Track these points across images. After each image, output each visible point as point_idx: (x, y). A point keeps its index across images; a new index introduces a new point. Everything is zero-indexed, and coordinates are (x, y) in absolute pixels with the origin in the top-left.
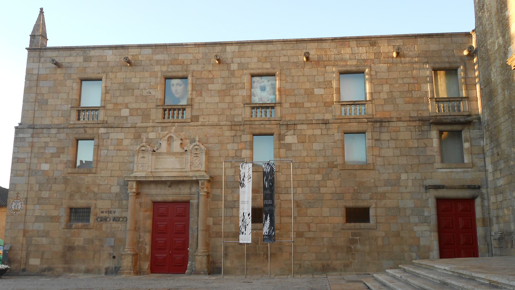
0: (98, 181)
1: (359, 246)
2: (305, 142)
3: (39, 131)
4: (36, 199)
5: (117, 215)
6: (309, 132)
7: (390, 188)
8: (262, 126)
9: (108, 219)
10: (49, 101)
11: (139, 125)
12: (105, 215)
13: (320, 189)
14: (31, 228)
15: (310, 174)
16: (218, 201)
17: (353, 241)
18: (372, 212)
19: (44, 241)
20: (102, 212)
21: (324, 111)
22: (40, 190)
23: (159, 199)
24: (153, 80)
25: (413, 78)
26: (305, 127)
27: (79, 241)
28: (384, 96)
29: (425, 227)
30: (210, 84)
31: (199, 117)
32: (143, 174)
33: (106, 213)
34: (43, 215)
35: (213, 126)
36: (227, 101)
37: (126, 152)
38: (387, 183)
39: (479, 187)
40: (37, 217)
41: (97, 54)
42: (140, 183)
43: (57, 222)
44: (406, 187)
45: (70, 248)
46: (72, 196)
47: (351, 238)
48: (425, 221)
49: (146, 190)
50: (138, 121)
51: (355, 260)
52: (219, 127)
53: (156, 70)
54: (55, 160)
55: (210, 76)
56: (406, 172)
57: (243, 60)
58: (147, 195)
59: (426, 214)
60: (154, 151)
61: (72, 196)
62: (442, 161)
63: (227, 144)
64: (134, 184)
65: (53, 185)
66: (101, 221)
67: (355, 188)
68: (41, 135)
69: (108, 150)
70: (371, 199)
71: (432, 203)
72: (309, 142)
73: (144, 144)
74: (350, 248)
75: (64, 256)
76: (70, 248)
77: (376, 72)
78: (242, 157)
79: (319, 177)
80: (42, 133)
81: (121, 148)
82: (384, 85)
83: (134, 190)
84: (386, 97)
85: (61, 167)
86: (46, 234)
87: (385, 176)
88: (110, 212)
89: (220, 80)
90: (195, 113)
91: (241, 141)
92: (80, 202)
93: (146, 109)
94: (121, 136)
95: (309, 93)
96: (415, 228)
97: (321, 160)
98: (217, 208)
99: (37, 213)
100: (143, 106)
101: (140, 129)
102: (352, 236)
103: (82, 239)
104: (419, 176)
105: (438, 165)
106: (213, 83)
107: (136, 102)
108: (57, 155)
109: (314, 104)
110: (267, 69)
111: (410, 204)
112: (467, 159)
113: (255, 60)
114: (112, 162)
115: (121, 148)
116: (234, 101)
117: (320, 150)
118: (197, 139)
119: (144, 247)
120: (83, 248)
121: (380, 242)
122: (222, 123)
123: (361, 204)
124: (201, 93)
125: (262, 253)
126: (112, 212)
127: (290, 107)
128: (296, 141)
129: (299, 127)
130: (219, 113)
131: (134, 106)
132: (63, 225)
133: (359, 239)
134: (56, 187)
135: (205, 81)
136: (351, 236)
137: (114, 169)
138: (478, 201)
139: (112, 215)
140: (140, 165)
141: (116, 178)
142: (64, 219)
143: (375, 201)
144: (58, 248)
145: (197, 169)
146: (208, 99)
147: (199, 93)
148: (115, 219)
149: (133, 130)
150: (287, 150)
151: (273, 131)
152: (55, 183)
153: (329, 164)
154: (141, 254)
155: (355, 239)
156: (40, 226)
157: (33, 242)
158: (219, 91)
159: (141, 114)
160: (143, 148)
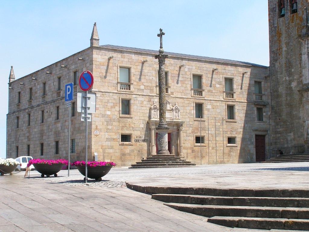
0: (134, 121)
1: (232, 153)
3: (104, 93)
4: (106, 130)
6: (215, 104)
14: (104, 144)
39: (267, 131)
45: (124, 155)
48: (252, 143)
54: (113, 110)
57: (190, 67)
68: (105, 96)
69: (137, 106)
70: (236, 134)
71: (254, 136)
75: (121, 158)
76: (124, 155)
86: (112, 147)
92: (126, 132)
96: (249, 146)
99: (107, 136)
100: (150, 85)
105: (256, 121)
107: (147, 82)
112: (264, 119)
113: (194, 67)
115: (143, 106)
120: (129, 154)
131: (145, 84)
134: (114, 123)
137: (141, 116)
138: (267, 136)
144: (118, 154)
156: (109, 143)
157: (106, 152)
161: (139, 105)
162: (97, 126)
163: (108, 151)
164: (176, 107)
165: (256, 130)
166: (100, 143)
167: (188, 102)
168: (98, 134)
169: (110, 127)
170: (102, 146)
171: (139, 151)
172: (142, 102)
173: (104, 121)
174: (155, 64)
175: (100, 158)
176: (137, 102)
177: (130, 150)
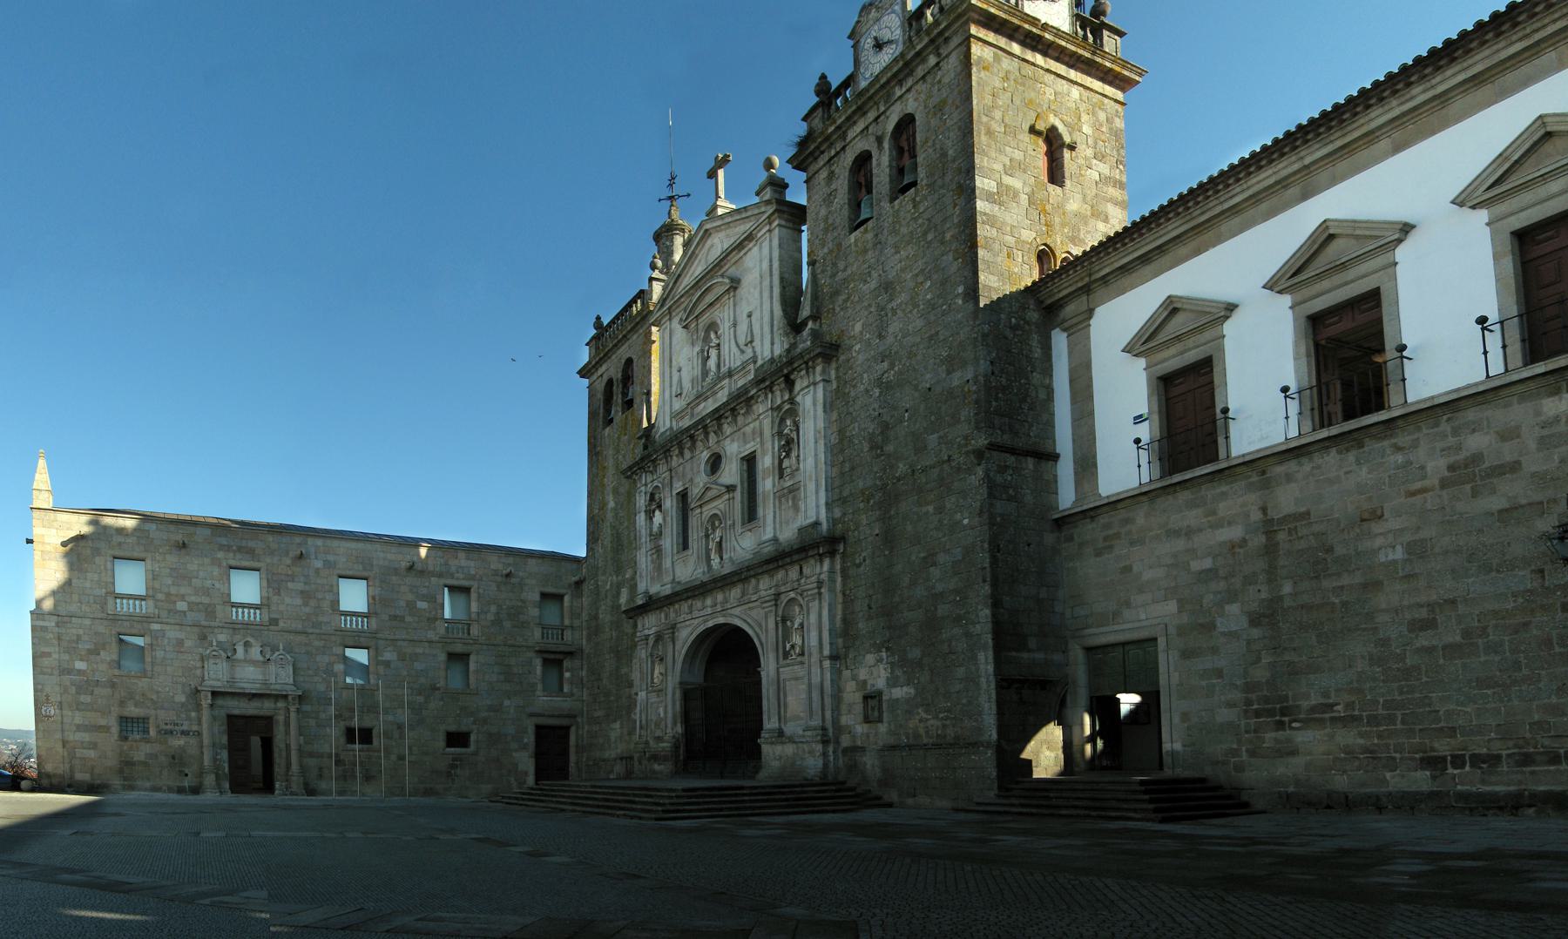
1: (458, 771)
5: (185, 728)
7: (492, 714)
11: (204, 623)
12: (169, 727)
17: (453, 766)
18: (473, 738)
20: (166, 724)
23: (236, 712)
26: (405, 644)
32: (219, 684)
42: (215, 694)
46: (122, 703)
48: (524, 747)
49: (220, 702)
50: (200, 617)
58: (222, 707)
59: (526, 740)
60: (228, 657)
61: (122, 703)
62: (544, 691)
64: (209, 694)
71: (531, 731)
79: (420, 699)
83: (209, 701)
85: (103, 667)
89: (302, 579)
90: (274, 616)
92: (133, 711)
93: (209, 605)
97: (422, 680)
100: (206, 600)
106: (293, 581)
108: (95, 652)
118: (281, 647)
120: (145, 764)
123: (464, 729)
129: (399, 643)
131: (193, 599)
132: (116, 736)
134: (97, 691)
141: (180, 687)
142: (115, 730)
146: (288, 600)
148: (183, 733)
149: (196, 629)
152: (97, 686)
158: (302, 592)
165: (532, 715)
171: (173, 757)
174: (220, 550)
176: (166, 641)
177: (146, 754)
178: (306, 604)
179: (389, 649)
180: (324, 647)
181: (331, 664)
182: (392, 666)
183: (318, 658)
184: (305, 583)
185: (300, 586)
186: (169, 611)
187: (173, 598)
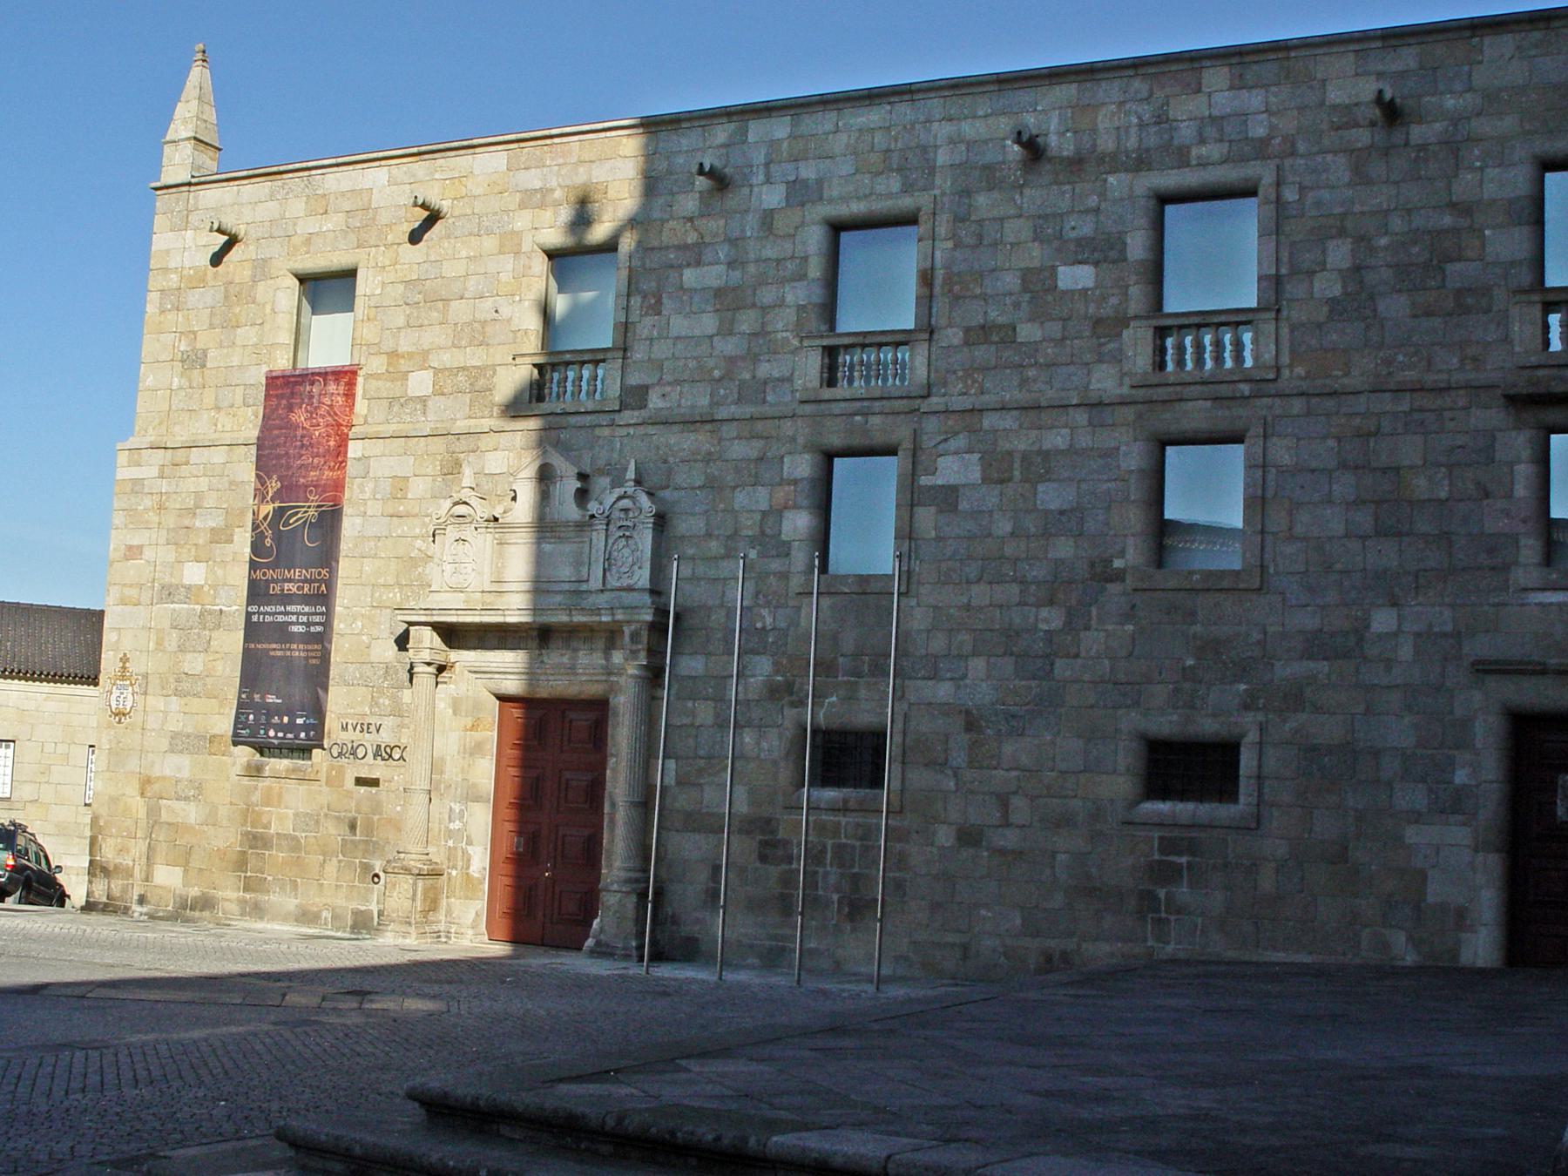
1: (1183, 892)
2: (1010, 479)
5: (385, 737)
7: (1324, 666)
8: (858, 418)
9: (361, 752)
10: (211, 354)
11: (461, 425)
13: (1052, 664)
14: (156, 772)
15: (1018, 604)
16: (695, 700)
17: (1165, 873)
18: (1247, 761)
19: (191, 813)
20: (345, 728)
21: (1088, 357)
22: (182, 649)
24: (508, 264)
25: (1453, 206)
26: (1007, 421)
27: (280, 821)
28: (1328, 286)
29: (1458, 834)
30: (689, 265)
31: (647, 392)
33: (355, 730)
34: (190, 730)
35: (691, 422)
36: (744, 328)
37: (416, 521)
38: (1316, 645)
40: (175, 736)
41: (346, 186)
43: (223, 755)
44: (1389, 664)
45: (257, 841)
47: (1157, 857)
48: (1454, 804)
51: (1168, 943)
52: (708, 427)
53: (519, 225)
55: (692, 238)
56: (1394, 604)
59: (1461, 777)
63: (734, 488)
65: (215, 634)
66: (340, 754)
67: (1190, 662)
68: (185, 470)
70: (1247, 707)
72: (1025, 480)
73: (465, 494)
74: (1155, 898)
75: (241, 863)
76: (257, 841)
77: (1302, 189)
78: (784, 537)
79: (1051, 619)
80: (187, 463)
81: (401, 508)
82: (1331, 245)
84: (1337, 291)
86: (196, 791)
87: (1308, 621)
88: (365, 728)
90: (634, 379)
91: (782, 479)
94: (405, 466)
95: (1038, 285)
96: (1412, 834)
97: (1064, 548)
98: (692, 725)
99: (174, 725)
100: (475, 357)
101: (458, 439)
102: (1162, 851)
103: (291, 812)
104: (1444, 619)
106: (698, 263)
109: (1055, 329)
110: (890, 195)
111: (1399, 732)
114: (375, 556)
116: (769, 329)
117: (1062, 513)
119: (464, 852)
121: (1267, 881)
122: (722, 413)
123: (1207, 727)
124: (659, 301)
125: (835, 897)
126: (373, 728)
127: (967, 343)
128: (975, 475)
129: (988, 421)
130: (717, 373)
131: (447, 359)
133: (1188, 862)
135: (672, 256)
136: (1159, 850)
137: (382, 581)
139: (370, 740)
140: (448, 568)
143: (1260, 717)
144: (227, 838)
145: (625, 582)
146: (679, 325)
147: (653, 301)
150: (941, 511)
151: (894, 438)
153: (1092, 565)
154: (454, 873)
155: (1174, 862)
157: (165, 817)
158: (719, 293)
159: (466, 386)
160: (461, 509)
161: (374, 508)
162: (125, 659)
163: (174, 811)
164: (620, 498)
166: (133, 764)
167: (750, 450)
168: (129, 704)
169: (194, 663)
170: (146, 782)
171: (353, 827)
172: (400, 486)
173: (166, 624)
175: (128, 851)
177: (296, 815)
178: (726, 330)
179: (953, 444)
180: (761, 459)
181: (775, 513)
182: (964, 505)
183: (741, 499)
184: (731, 264)
185: (713, 275)
186: (392, 401)
187: (403, 365)
